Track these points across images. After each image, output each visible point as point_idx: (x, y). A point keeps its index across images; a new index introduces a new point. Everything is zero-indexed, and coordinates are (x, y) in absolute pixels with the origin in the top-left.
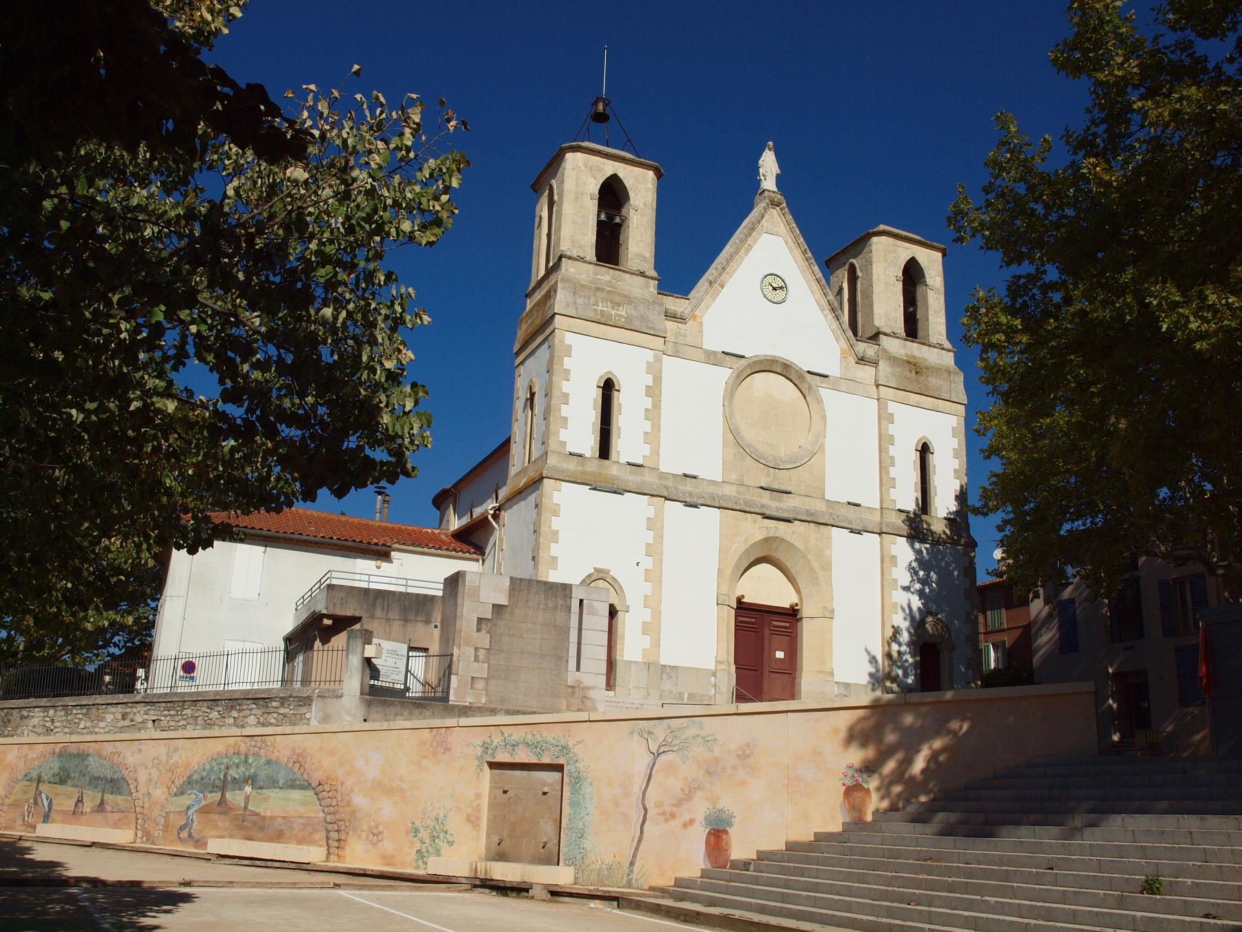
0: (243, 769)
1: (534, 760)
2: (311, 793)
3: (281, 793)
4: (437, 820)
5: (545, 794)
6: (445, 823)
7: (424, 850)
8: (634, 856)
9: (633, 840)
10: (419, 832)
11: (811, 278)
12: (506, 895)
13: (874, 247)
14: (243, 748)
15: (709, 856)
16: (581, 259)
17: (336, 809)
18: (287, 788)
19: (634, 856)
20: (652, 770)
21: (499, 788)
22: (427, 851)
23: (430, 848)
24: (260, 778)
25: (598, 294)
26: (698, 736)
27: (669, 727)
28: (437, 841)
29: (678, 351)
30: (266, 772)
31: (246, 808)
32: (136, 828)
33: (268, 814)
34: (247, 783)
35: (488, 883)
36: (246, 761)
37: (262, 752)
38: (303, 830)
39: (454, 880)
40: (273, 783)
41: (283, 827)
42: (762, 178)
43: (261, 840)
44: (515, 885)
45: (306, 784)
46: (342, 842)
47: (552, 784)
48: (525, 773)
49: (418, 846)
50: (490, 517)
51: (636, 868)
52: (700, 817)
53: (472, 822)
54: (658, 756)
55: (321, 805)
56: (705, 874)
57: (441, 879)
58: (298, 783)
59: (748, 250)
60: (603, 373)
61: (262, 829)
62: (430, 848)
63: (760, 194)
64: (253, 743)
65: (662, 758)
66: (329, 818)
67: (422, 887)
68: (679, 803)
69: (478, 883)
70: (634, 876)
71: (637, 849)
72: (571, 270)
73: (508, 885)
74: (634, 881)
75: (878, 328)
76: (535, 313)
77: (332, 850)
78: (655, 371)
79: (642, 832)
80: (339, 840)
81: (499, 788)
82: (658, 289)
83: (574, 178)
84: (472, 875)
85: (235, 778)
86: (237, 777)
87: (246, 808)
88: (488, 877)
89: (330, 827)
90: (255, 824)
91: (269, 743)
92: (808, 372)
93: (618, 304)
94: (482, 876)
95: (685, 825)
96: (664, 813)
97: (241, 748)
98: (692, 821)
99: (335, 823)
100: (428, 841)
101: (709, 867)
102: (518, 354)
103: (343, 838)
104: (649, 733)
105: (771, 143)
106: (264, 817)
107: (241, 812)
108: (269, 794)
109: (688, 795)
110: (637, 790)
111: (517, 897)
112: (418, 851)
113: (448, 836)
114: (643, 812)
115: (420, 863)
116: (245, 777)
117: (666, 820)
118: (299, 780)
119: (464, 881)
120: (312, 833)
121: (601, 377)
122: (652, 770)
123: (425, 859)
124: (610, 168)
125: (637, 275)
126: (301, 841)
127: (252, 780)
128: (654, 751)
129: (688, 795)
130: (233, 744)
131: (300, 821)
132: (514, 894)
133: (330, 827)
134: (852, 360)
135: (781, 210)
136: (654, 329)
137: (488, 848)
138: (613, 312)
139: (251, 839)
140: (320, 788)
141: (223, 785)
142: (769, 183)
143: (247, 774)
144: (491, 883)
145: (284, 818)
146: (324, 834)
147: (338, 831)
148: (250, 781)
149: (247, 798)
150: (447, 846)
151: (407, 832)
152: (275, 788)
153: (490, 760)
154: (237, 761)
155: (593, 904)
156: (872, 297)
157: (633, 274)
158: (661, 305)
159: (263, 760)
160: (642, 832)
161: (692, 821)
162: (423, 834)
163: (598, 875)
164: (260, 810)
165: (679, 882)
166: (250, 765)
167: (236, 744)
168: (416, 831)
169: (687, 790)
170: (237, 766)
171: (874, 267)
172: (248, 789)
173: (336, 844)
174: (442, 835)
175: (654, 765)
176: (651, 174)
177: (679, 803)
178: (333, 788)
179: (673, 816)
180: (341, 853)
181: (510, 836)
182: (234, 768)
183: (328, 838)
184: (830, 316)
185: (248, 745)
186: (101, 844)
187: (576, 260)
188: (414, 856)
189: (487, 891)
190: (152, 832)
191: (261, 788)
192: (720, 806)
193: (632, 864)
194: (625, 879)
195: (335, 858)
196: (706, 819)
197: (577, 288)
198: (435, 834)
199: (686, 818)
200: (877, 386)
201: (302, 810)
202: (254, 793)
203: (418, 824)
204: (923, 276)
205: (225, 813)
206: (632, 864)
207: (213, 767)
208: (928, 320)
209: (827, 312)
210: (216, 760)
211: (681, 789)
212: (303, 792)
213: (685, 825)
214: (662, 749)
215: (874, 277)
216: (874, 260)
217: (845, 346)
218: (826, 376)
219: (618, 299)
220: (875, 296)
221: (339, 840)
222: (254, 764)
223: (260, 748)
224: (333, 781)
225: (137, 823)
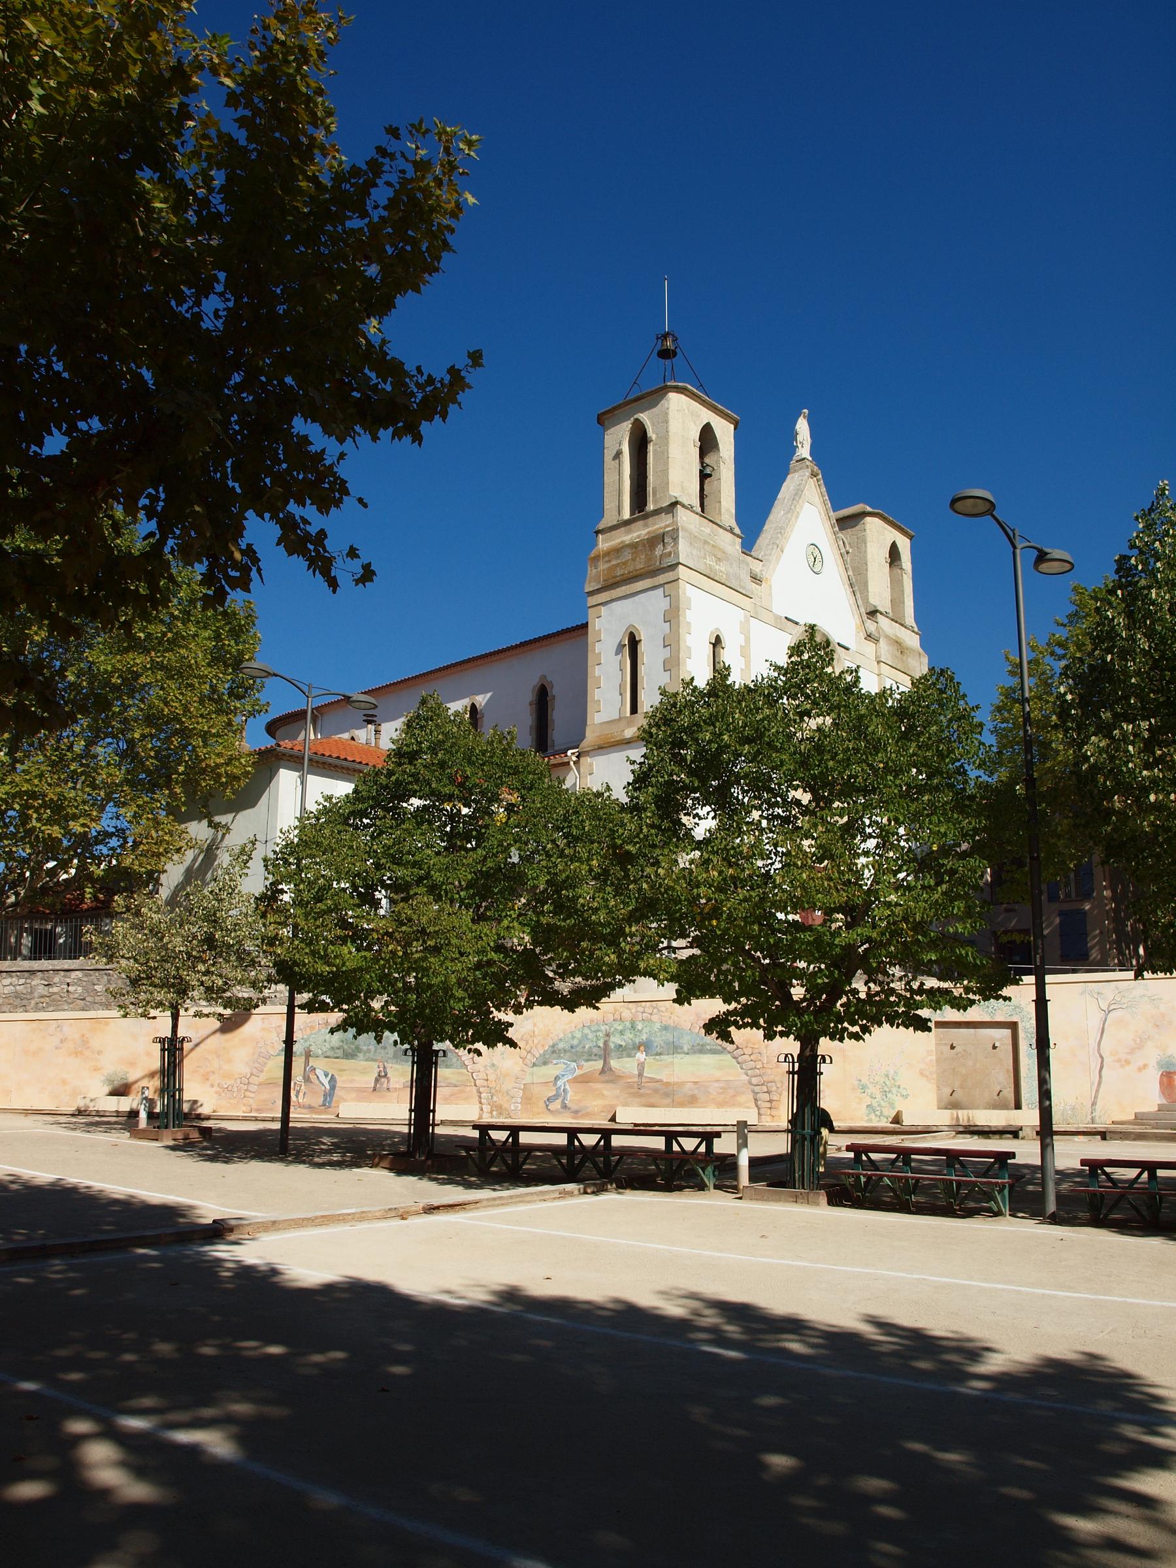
0: (631, 1036)
1: (987, 1019)
2: (729, 1057)
3: (688, 1058)
4: (887, 1076)
5: (994, 1047)
6: (897, 1078)
7: (875, 1104)
8: (1096, 1097)
9: (1092, 1084)
10: (868, 1088)
11: (837, 552)
12: (989, 1138)
13: (868, 527)
14: (627, 1014)
15: (1163, 1094)
16: (690, 508)
17: (762, 1071)
18: (694, 1053)
19: (1096, 1097)
20: (1104, 1024)
21: (946, 1044)
22: (879, 1105)
23: (882, 1103)
24: (655, 1044)
25: (706, 547)
26: (1144, 995)
27: (1117, 988)
28: (889, 1095)
29: (756, 612)
30: (664, 1038)
31: (640, 1075)
32: (481, 1103)
33: (671, 1080)
34: (639, 1048)
35: (972, 1129)
36: (633, 1027)
37: (655, 1018)
38: (723, 1093)
39: (935, 1129)
40: (674, 1048)
41: (696, 1092)
42: (800, 445)
43: (668, 1106)
44: (1001, 1129)
45: (719, 1048)
46: (774, 1103)
47: (1000, 1040)
48: (972, 1031)
49: (868, 1101)
50: (572, 763)
51: (1098, 1107)
52: (1152, 1063)
53: (927, 1077)
54: (1109, 1012)
55: (742, 1068)
56: (1161, 1108)
57: (920, 1129)
58: (708, 1047)
59: (797, 517)
60: (712, 628)
61: (666, 1095)
62: (882, 1103)
63: (797, 461)
64: (641, 1009)
65: (1112, 1014)
66: (754, 1080)
67: (914, 1139)
68: (1132, 1051)
69: (961, 1129)
70: (1097, 1114)
71: (1097, 1091)
72: (685, 519)
73: (993, 1129)
74: (1097, 1118)
75: (875, 607)
76: (627, 555)
77: (762, 1111)
78: (746, 631)
79: (1100, 1077)
80: (770, 1101)
81: (946, 1044)
82: (742, 547)
83: (681, 420)
84: (954, 1123)
85: (621, 1046)
86: (623, 1044)
87: (640, 1075)
88: (972, 1123)
89: (757, 1089)
90: (656, 1091)
91: (663, 1009)
92: (839, 644)
93: (720, 560)
94: (965, 1123)
95: (1140, 1070)
96: (1119, 1061)
97: (623, 1015)
98: (1145, 1066)
99: (762, 1085)
100: (879, 1096)
101: (1164, 1102)
102: (591, 593)
103: (775, 1098)
104: (1098, 993)
105: (806, 411)
106: (668, 1084)
107: (636, 1080)
108: (671, 1060)
109: (1139, 1044)
110: (1093, 1042)
111: (1001, 1138)
112: (867, 1106)
113: (901, 1090)
114: (1100, 1060)
115: (872, 1116)
116: (634, 1044)
117: (1122, 1066)
118: (708, 1044)
119: (946, 1129)
120: (734, 1096)
121: (712, 633)
122: (1104, 1024)
123: (877, 1113)
124: (707, 416)
125: (727, 530)
126: (720, 1105)
127: (646, 1046)
128: (1105, 1009)
129: (1139, 1044)
130: (612, 1011)
131: (716, 1085)
132: (997, 1136)
133: (757, 1089)
134: (863, 635)
135: (818, 481)
136: (744, 588)
137: (939, 1100)
138: (717, 567)
139: (652, 1106)
140: (739, 1052)
141: (605, 1053)
142: (804, 451)
143: (637, 1041)
144: (975, 1129)
145: (695, 1083)
146: (751, 1096)
147: (768, 1092)
148: (642, 1048)
149: (641, 1066)
150: (901, 1099)
151: (853, 1089)
152: (679, 1053)
153: (940, 1019)
154: (620, 1028)
155: (1077, 1138)
156: (866, 575)
157: (725, 529)
158: (748, 564)
159: (658, 1025)
160: (1100, 1077)
161: (1145, 1066)
162: (872, 1089)
163: (1063, 1115)
164: (664, 1076)
165: (1139, 1118)
166: (640, 1031)
167: (616, 1010)
168: (864, 1087)
169: (1138, 1042)
170: (622, 1033)
171: (868, 545)
172: (641, 1056)
173: (768, 1105)
174: (894, 1090)
175: (1106, 1020)
176: (732, 427)
177: (1132, 1051)
178: (756, 1051)
179: (1128, 1062)
180: (774, 1112)
181: (962, 1087)
182: (618, 1035)
183: (756, 1100)
184: (849, 590)
185: (633, 1011)
186: (452, 1121)
187: (687, 508)
188: (864, 1110)
189: (968, 1136)
190: (505, 1105)
191: (660, 1054)
192: (1169, 1053)
193: (1094, 1104)
194: (1089, 1117)
195: (769, 1119)
196: (1158, 1063)
197: (693, 539)
198: (886, 1089)
199: (1141, 1064)
200: (878, 662)
201: (718, 1074)
202: (650, 1059)
203: (865, 1081)
204: (900, 560)
205: (612, 1082)
206: (1094, 1104)
207: (586, 1035)
208: (903, 603)
209: (847, 586)
210: (589, 1027)
211: (1133, 1040)
212: (717, 1057)
213: (1140, 1070)
214: (1112, 1007)
215: (869, 556)
216: (869, 539)
217: (858, 621)
218: (847, 649)
219: (720, 555)
220: (870, 575)
221: (770, 1101)
222: (644, 1031)
223: (651, 1014)
224: (754, 1044)
225: (480, 1097)
